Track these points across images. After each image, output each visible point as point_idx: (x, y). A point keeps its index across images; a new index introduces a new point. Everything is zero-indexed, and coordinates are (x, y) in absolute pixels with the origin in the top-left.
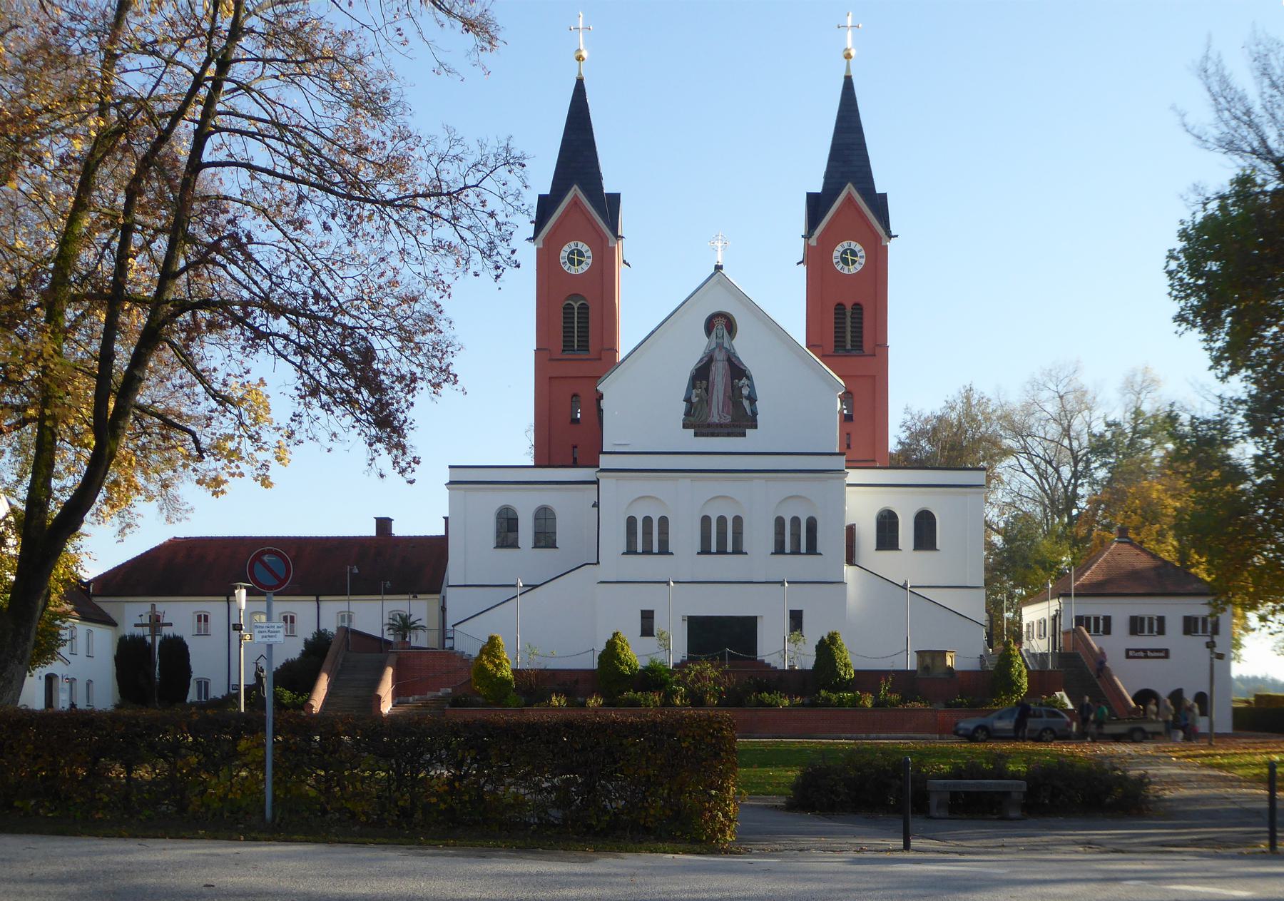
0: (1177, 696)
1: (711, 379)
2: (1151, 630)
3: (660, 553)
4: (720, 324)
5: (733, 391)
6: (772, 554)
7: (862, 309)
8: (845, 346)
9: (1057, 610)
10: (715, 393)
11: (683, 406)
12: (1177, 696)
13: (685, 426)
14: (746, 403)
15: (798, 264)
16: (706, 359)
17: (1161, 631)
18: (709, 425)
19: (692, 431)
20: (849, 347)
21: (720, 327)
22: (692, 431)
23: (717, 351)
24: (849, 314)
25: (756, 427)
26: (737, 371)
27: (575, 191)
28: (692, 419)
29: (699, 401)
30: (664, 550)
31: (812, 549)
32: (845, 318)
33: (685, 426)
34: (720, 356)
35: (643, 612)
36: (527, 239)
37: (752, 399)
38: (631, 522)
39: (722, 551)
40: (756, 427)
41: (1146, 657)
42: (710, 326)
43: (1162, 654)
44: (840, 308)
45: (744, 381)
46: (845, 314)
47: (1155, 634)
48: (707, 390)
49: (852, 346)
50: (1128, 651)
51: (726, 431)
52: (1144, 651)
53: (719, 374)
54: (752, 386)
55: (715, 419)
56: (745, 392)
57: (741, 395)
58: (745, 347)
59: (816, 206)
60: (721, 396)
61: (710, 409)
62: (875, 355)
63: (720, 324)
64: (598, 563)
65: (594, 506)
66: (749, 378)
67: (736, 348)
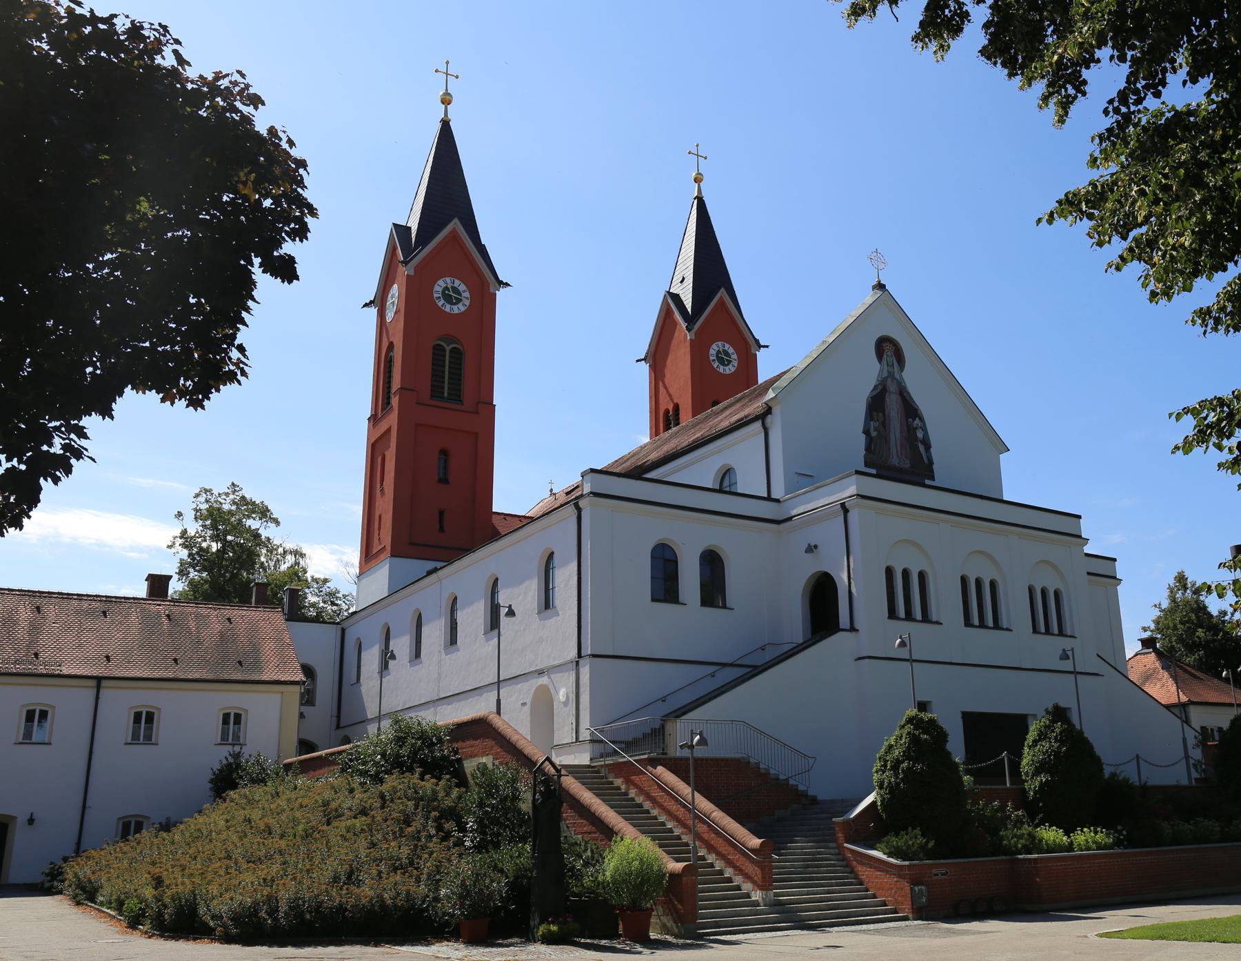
1: (887, 413)
4: (889, 351)
5: (908, 431)
11: (863, 438)
14: (922, 448)
16: (880, 387)
23: (889, 380)
26: (911, 410)
37: (928, 447)
45: (917, 421)
48: (884, 424)
54: (924, 429)
55: (895, 461)
56: (920, 434)
58: (914, 379)
60: (898, 435)
61: (890, 449)
63: (889, 351)
66: (922, 420)
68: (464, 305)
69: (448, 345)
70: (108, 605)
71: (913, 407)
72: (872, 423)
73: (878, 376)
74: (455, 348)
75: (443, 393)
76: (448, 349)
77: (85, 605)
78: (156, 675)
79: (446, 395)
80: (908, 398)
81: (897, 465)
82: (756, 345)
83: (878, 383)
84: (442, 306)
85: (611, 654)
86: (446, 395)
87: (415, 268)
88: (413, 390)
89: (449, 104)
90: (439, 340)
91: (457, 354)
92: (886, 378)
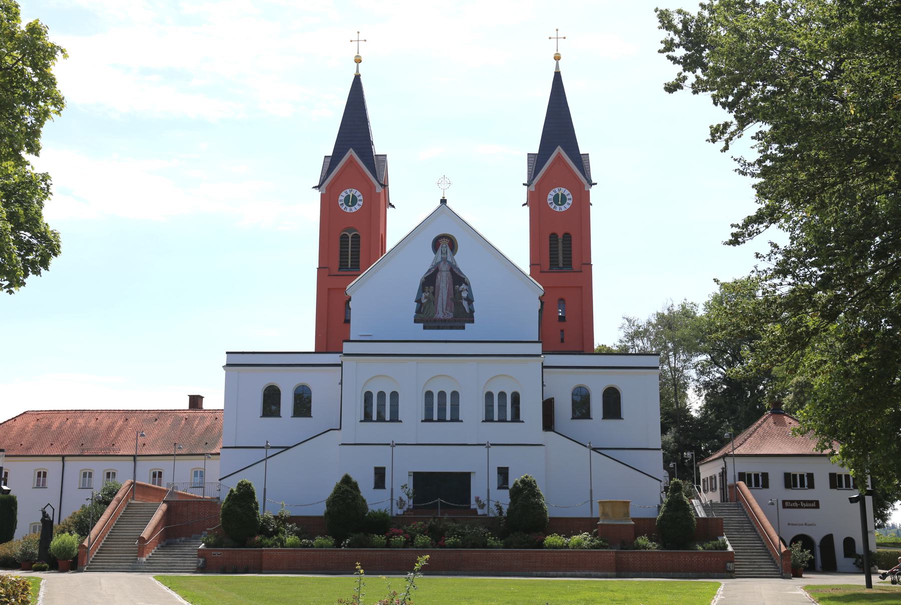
0: (828, 540)
2: (802, 485)
3: (391, 421)
4: (444, 244)
6: (483, 421)
7: (571, 237)
8: (558, 265)
9: (723, 468)
10: (440, 295)
12: (828, 540)
13: (416, 321)
14: (465, 303)
15: (523, 205)
16: (433, 269)
17: (811, 486)
18: (435, 321)
19: (421, 325)
20: (561, 265)
21: (444, 246)
22: (421, 325)
24: (560, 241)
25: (473, 322)
26: (458, 279)
27: (351, 152)
28: (422, 316)
29: (427, 302)
30: (395, 419)
31: (516, 418)
32: (557, 244)
33: (416, 321)
34: (444, 267)
35: (376, 469)
36: (314, 187)
37: (470, 300)
38: (368, 396)
39: (442, 419)
40: (473, 322)
41: (800, 507)
42: (436, 244)
43: (814, 505)
44: (553, 237)
45: (463, 286)
46: (557, 240)
47: (806, 488)
48: (434, 293)
49: (564, 264)
50: (784, 502)
51: (449, 325)
52: (799, 502)
53: (444, 280)
54: (469, 290)
55: (440, 315)
56: (464, 294)
57: (461, 298)
58: (463, 261)
59: (537, 162)
60: (445, 298)
62: (581, 272)
63: (444, 244)
64: (341, 428)
65: (339, 384)
66: (467, 284)
67: (456, 260)
68: (359, 205)
69: (350, 234)
70: (160, 415)
71: (462, 278)
72: (423, 294)
73: (433, 263)
74: (354, 234)
75: (348, 265)
76: (350, 236)
77: (150, 415)
78: (161, 453)
79: (349, 266)
80: (457, 272)
81: (442, 318)
82: (588, 184)
83: (432, 267)
84: (344, 209)
85: (234, 446)
86: (349, 266)
87: (326, 188)
88: (326, 268)
89: (361, 62)
90: (344, 231)
91: (356, 238)
92: (440, 262)
